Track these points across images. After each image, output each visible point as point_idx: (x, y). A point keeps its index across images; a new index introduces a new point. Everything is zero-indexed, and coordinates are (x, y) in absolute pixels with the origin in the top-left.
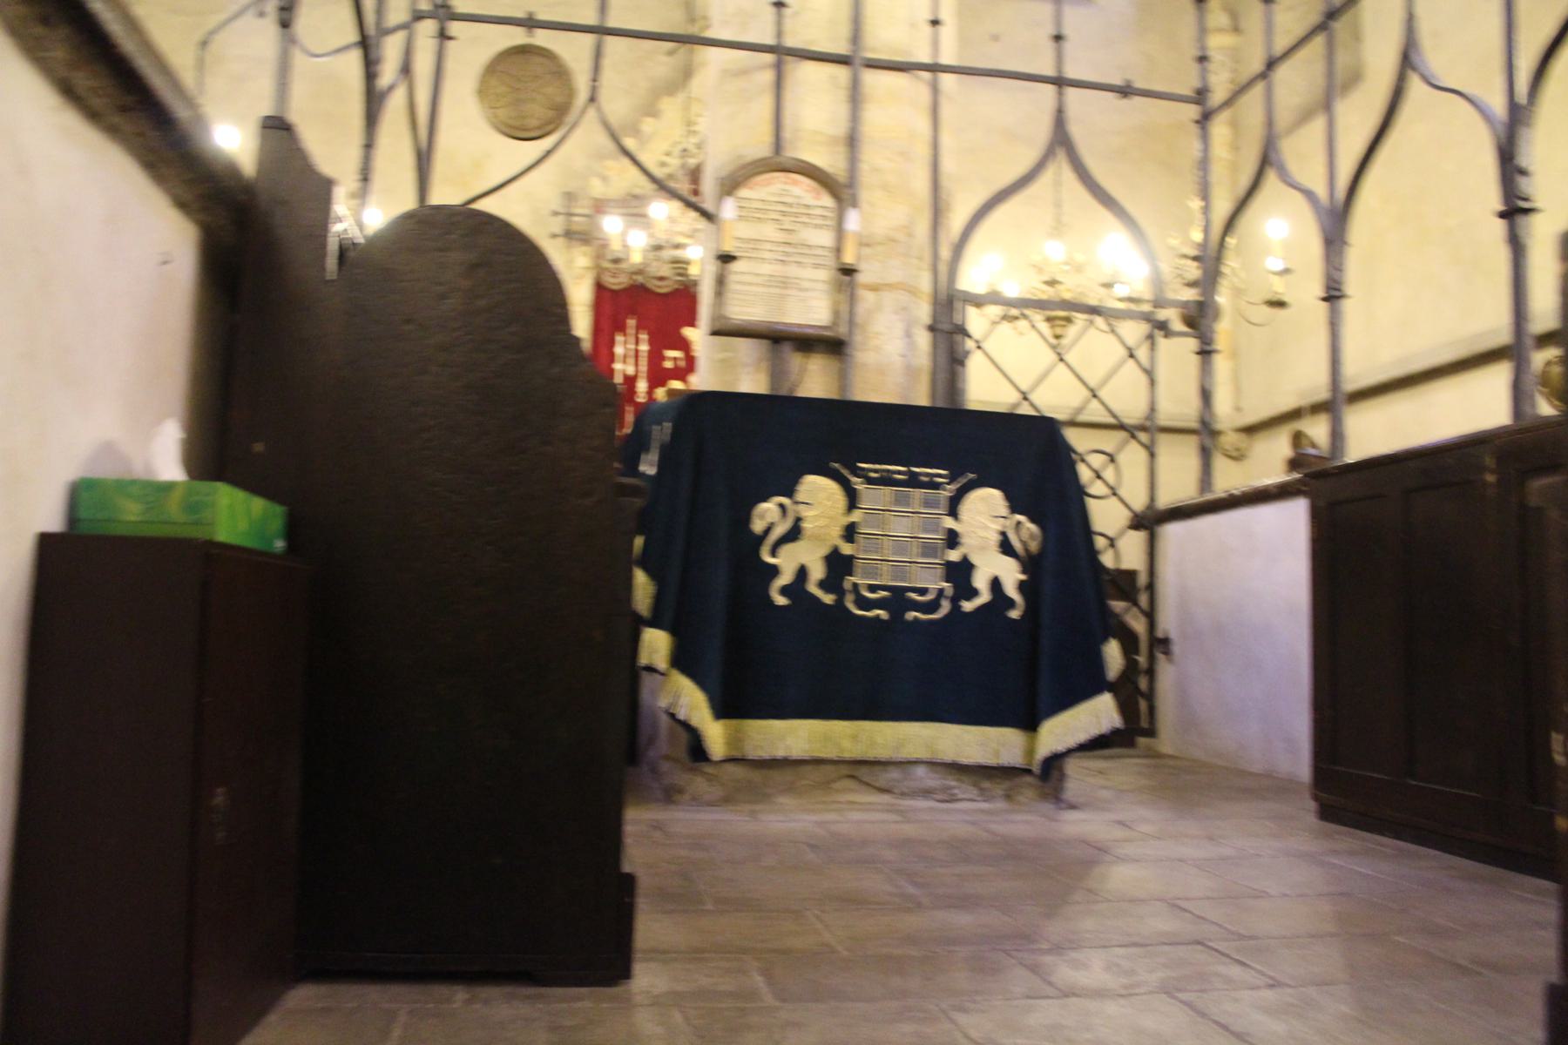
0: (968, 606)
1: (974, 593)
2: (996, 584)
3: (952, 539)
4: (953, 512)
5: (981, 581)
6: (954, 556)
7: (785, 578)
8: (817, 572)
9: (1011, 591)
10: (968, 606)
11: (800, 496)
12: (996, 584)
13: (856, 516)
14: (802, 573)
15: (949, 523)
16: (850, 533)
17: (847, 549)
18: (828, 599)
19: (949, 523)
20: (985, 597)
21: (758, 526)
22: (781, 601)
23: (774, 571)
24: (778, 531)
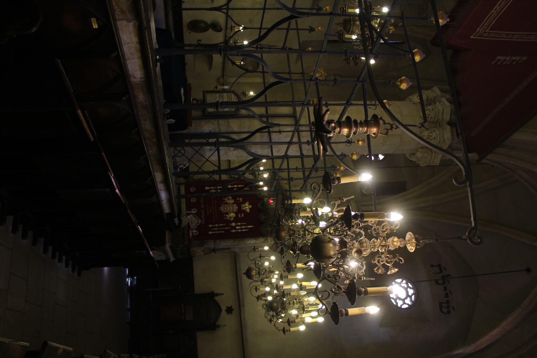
0: (224, 215)
1: (226, 215)
2: (227, 217)
3: (230, 213)
4: (233, 212)
5: (227, 215)
6: (229, 213)
7: (225, 199)
8: (226, 202)
9: (226, 218)
10: (224, 215)
11: (232, 200)
12: (227, 217)
13: (231, 204)
14: (226, 201)
15: (231, 212)
16: (230, 203)
17: (228, 203)
18: (224, 203)
19: (231, 212)
20: (226, 216)
21: (229, 197)
22: (223, 199)
23: (225, 198)
24: (229, 198)
